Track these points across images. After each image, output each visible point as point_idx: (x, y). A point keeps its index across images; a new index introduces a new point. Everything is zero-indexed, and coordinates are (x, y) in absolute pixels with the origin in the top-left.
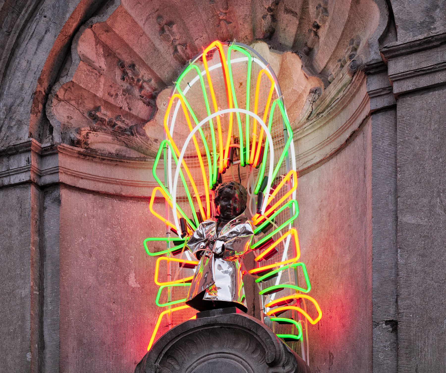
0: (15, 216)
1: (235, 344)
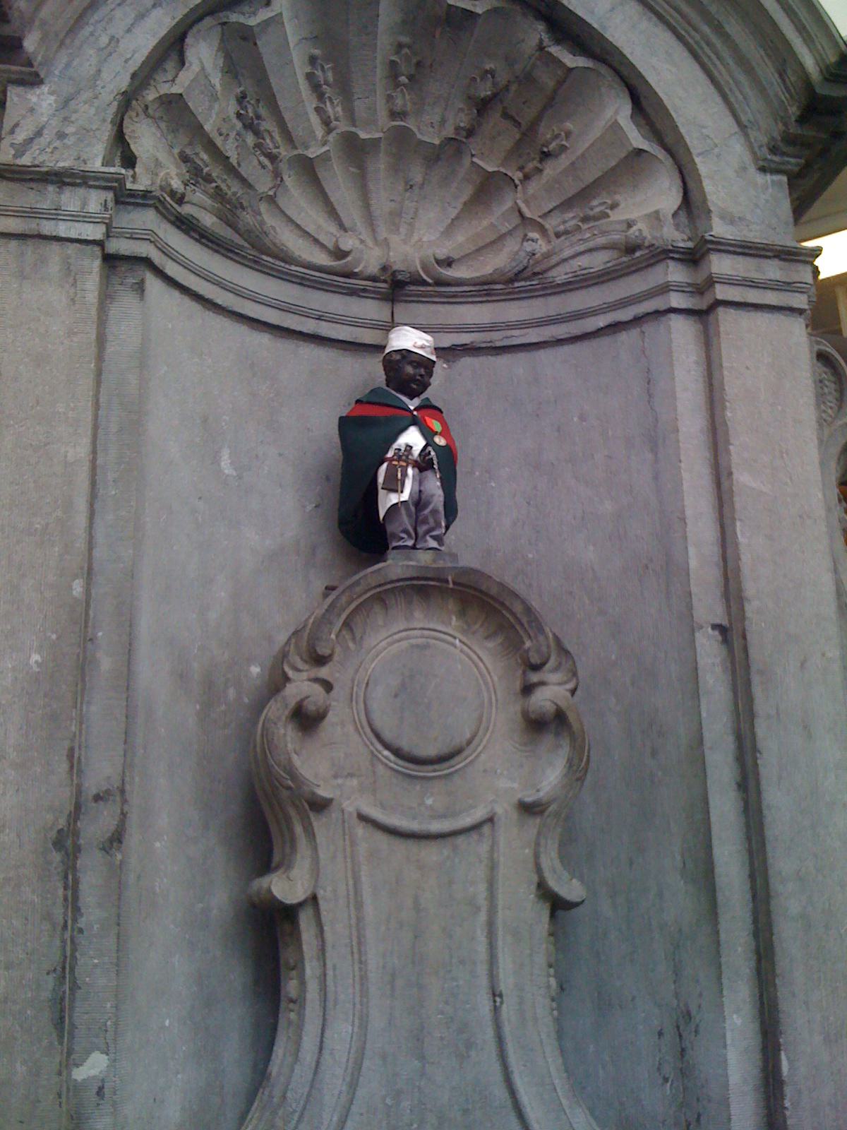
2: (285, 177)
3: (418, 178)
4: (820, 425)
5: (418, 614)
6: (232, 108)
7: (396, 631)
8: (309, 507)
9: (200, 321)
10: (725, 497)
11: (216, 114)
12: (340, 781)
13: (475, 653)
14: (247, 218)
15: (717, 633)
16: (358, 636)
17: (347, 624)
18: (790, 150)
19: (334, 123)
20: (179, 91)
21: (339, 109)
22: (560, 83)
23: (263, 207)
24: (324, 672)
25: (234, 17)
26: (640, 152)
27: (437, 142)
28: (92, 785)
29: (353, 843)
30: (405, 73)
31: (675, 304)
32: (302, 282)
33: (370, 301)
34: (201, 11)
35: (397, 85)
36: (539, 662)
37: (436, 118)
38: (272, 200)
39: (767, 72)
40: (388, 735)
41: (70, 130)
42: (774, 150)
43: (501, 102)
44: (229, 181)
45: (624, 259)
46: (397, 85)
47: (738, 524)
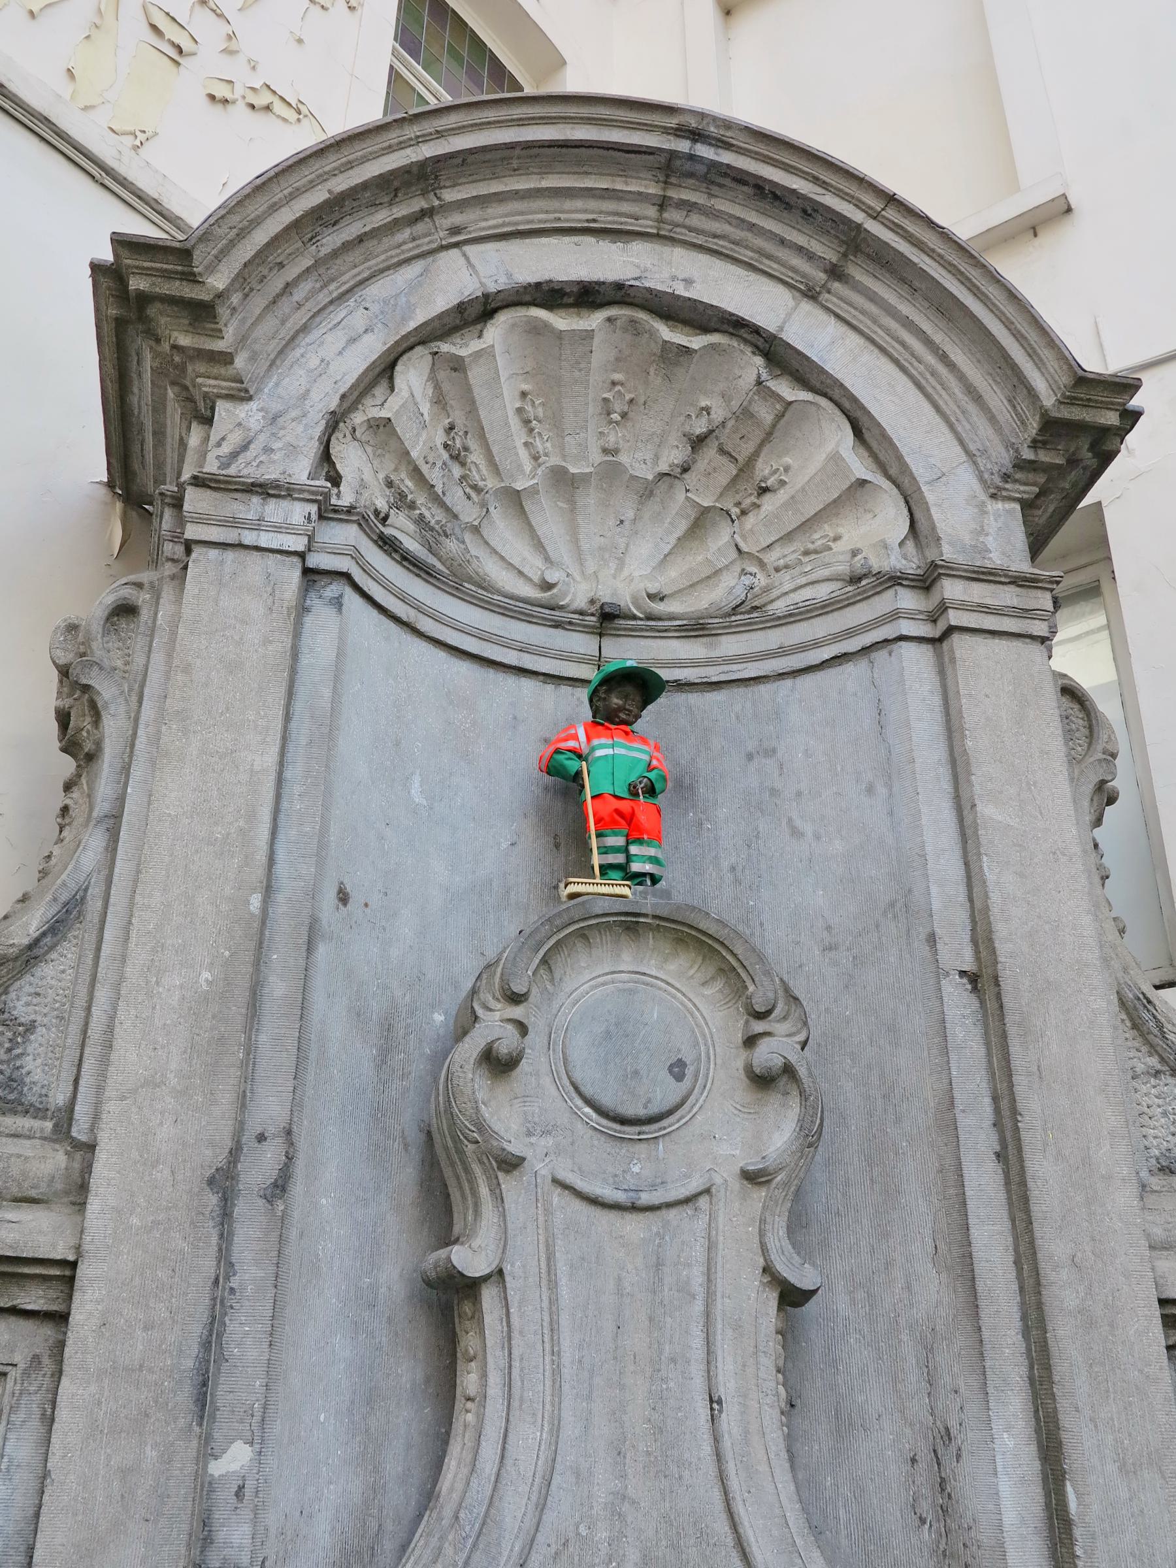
0: (256, 608)
1: (666, 960)
2: (492, 509)
3: (630, 514)
4: (1069, 762)
6: (440, 438)
7: (601, 972)
9: (396, 644)
10: (969, 832)
11: (423, 440)
12: (533, 1139)
13: (690, 1000)
14: (451, 546)
15: (965, 980)
16: (557, 975)
17: (545, 961)
20: (388, 416)
22: (780, 416)
23: (468, 537)
24: (517, 1012)
25: (445, 347)
26: (863, 483)
27: (650, 477)
28: (254, 1126)
29: (548, 1212)
30: (618, 410)
31: (905, 633)
32: (505, 612)
34: (412, 340)
36: (763, 1010)
37: (649, 456)
38: (476, 530)
39: (996, 399)
40: (588, 1091)
42: (1006, 477)
43: (717, 438)
44: (434, 510)
45: (850, 588)
46: (611, 422)
47: (985, 858)
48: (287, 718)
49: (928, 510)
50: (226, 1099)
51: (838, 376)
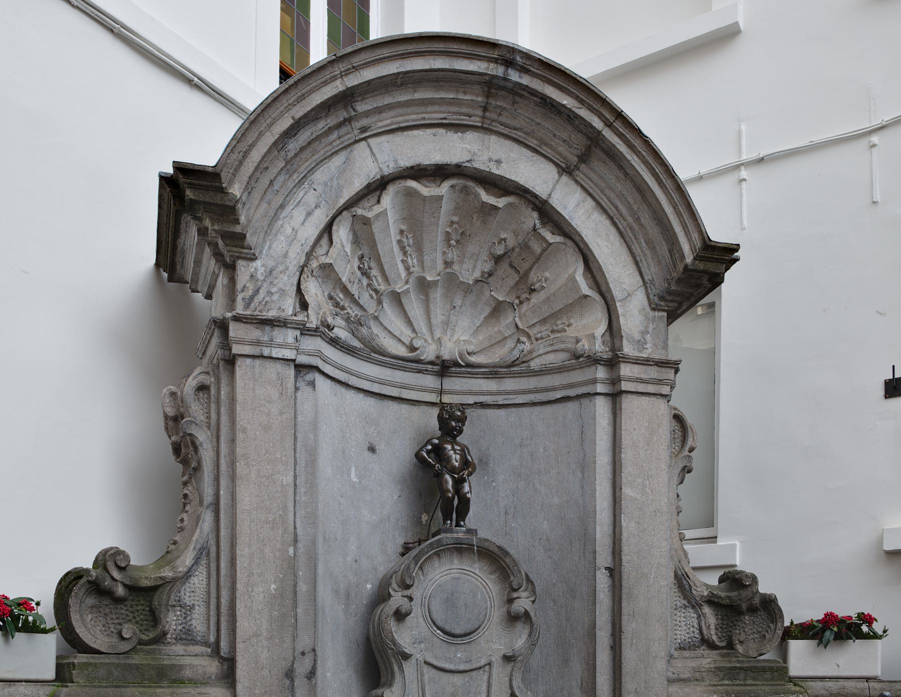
5: (456, 561)
6: (356, 263)
8: (396, 497)
18: (670, 298)
19: (412, 269)
21: (415, 261)
23: (372, 323)
27: (471, 282)
33: (429, 376)
35: (450, 246)
37: (471, 267)
41: (274, 290)
46: (450, 246)
48: (295, 452)
49: (618, 318)
50: (288, 640)
51: (579, 230)
